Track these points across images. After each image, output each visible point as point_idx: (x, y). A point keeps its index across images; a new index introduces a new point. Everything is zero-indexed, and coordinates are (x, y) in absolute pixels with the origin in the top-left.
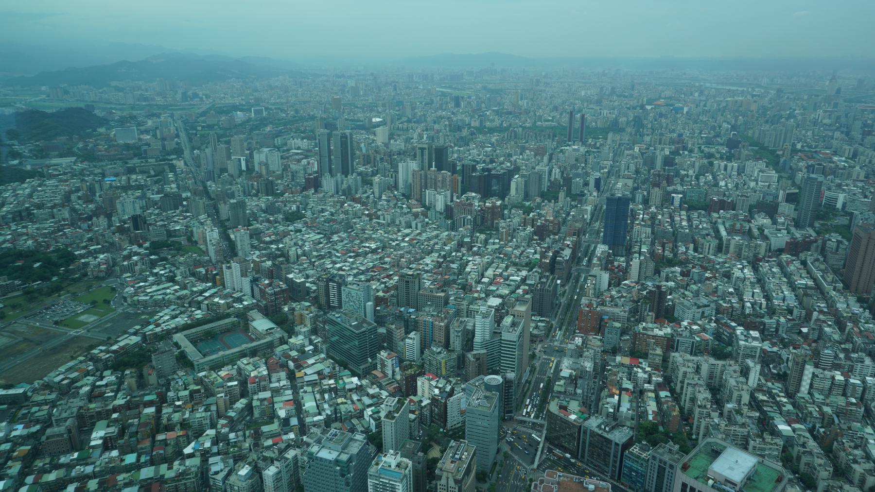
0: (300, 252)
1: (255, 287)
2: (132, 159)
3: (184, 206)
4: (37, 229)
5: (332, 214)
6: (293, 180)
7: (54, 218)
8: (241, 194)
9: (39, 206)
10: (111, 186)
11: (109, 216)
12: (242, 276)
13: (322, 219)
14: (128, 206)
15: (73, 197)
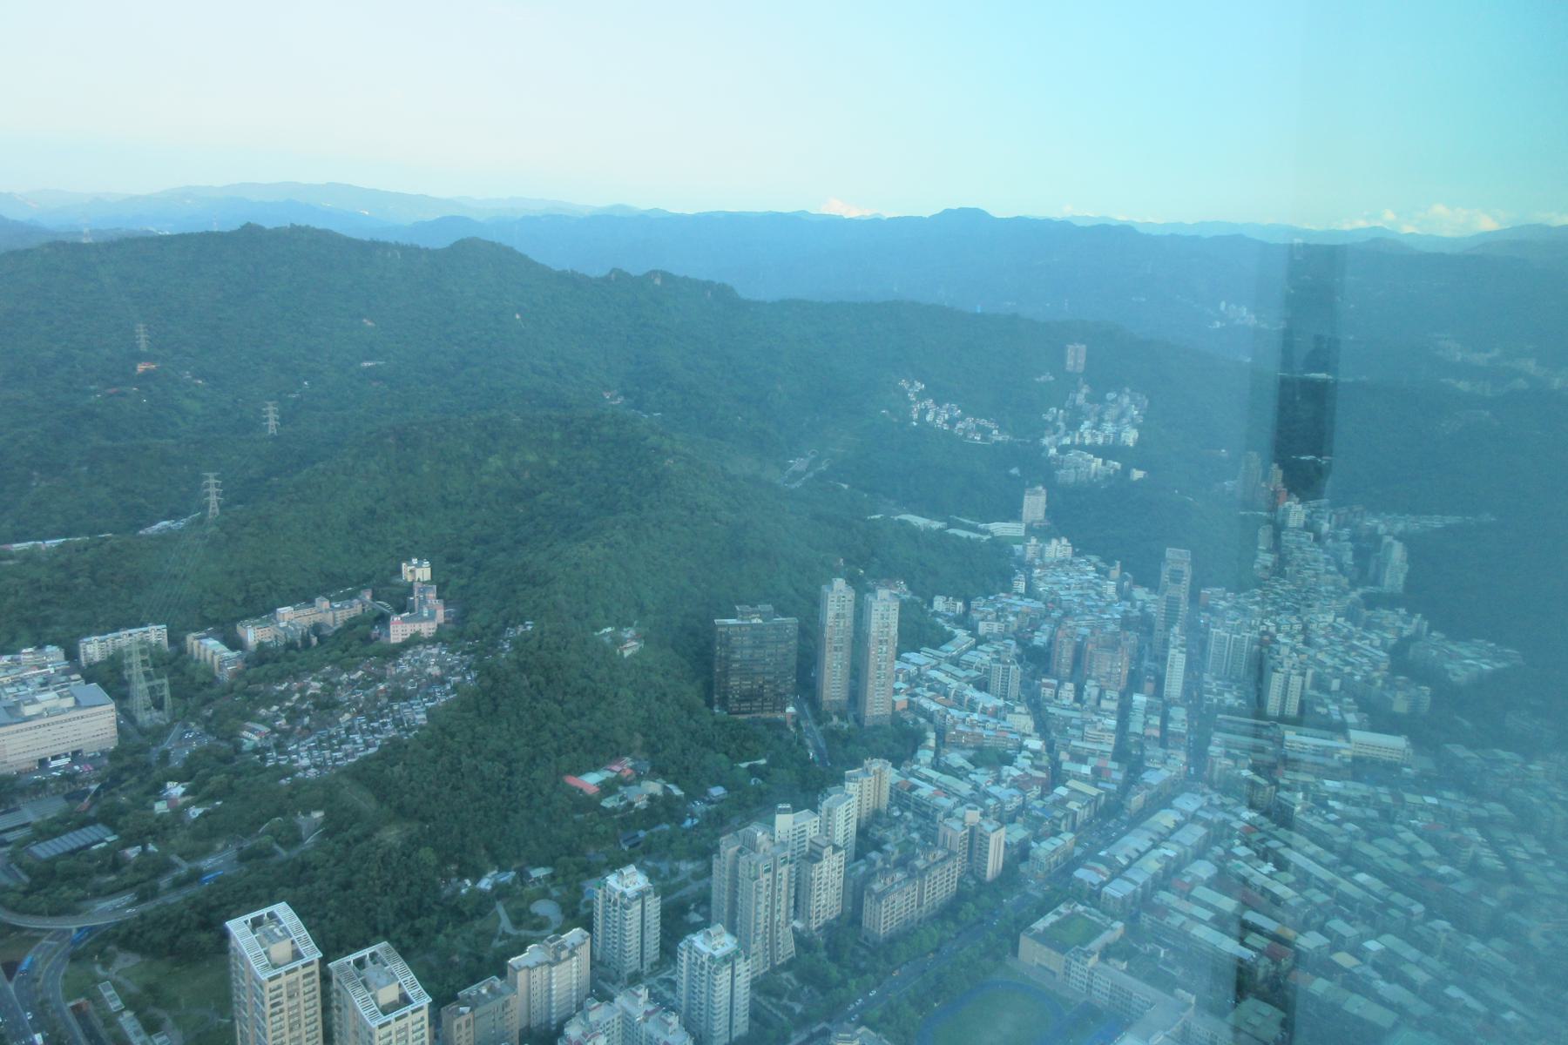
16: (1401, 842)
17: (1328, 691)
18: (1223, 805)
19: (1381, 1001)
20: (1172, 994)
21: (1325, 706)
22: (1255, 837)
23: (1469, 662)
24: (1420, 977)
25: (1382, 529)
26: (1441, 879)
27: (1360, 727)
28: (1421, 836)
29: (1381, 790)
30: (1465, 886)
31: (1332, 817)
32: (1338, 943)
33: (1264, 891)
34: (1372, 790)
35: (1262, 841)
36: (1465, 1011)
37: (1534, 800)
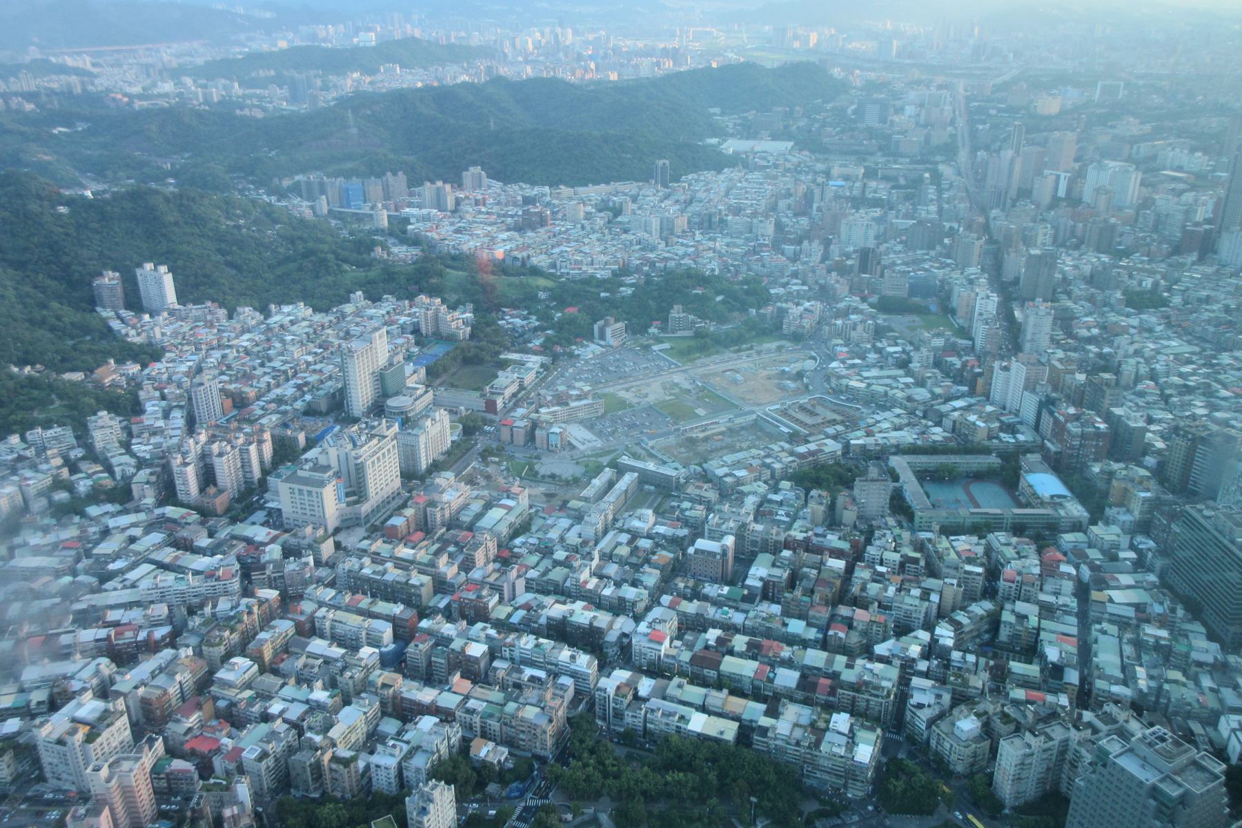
0: (1143, 370)
1: (1045, 416)
2: (872, 154)
3: (944, 246)
4: (728, 245)
5: (1227, 310)
6: (1155, 229)
7: (751, 231)
8: (1048, 240)
9: (737, 211)
10: (837, 197)
11: (827, 243)
12: (1025, 389)
13: (1206, 315)
14: (859, 229)
15: (782, 204)
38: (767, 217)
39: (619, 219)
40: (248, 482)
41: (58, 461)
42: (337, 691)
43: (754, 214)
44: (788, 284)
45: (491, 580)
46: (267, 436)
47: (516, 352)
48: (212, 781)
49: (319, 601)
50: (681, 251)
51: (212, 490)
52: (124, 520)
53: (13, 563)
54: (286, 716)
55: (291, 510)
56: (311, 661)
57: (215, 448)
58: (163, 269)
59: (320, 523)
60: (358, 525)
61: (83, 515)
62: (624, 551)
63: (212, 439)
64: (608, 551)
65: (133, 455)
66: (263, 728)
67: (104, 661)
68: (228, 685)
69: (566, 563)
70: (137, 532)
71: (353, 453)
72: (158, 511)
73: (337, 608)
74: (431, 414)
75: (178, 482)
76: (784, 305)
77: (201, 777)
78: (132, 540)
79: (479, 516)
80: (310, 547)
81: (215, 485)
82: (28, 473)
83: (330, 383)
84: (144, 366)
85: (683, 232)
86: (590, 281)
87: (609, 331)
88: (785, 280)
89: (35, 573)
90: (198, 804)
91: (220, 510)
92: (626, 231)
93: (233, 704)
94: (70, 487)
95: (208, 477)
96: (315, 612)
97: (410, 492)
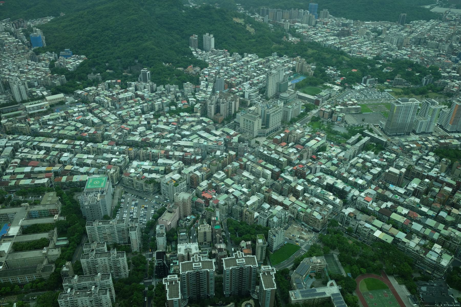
7: (437, 48)
16: (72, 126)
17: (34, 86)
18: (14, 138)
19: (82, 174)
20: (21, 206)
21: (35, 92)
22: (28, 144)
23: (73, 63)
24: (89, 162)
25: (32, 25)
26: (86, 131)
27: (47, 95)
28: (76, 121)
29: (62, 112)
30: (92, 131)
31: (50, 127)
32: (64, 164)
33: (37, 159)
34: (59, 113)
35: (31, 144)
36: (103, 165)
37: (102, 98)
38: (447, 42)
39: (380, 36)
40: (230, 114)
41: (174, 96)
42: (250, 190)
43: (441, 41)
44: (450, 72)
45: (308, 165)
46: (238, 99)
47: (330, 83)
48: (209, 208)
49: (248, 158)
50: (404, 52)
51: (218, 114)
52: (191, 119)
53: (158, 126)
54: (233, 194)
55: (243, 126)
56: (243, 178)
57: (221, 100)
58: (212, 36)
59: (252, 132)
60: (264, 136)
61: (179, 115)
62: (359, 165)
63: (220, 98)
64: (353, 164)
65: (195, 98)
66: (226, 196)
67: (181, 162)
68: (217, 179)
69: (337, 165)
70: (194, 124)
71: (267, 111)
72: (201, 118)
73: (254, 163)
74: (296, 101)
75: (208, 109)
76: (446, 81)
77: (205, 206)
78: (192, 126)
79: (308, 141)
80: (247, 140)
81: (220, 113)
82: (165, 98)
83: (261, 84)
84: (202, 69)
85: (407, 44)
86: (365, 60)
87: (368, 80)
88: (448, 70)
89: (163, 130)
90: (204, 213)
91: (220, 122)
92: (382, 42)
93: (217, 186)
94: (176, 106)
95: (218, 110)
96: (247, 162)
97: (284, 127)
